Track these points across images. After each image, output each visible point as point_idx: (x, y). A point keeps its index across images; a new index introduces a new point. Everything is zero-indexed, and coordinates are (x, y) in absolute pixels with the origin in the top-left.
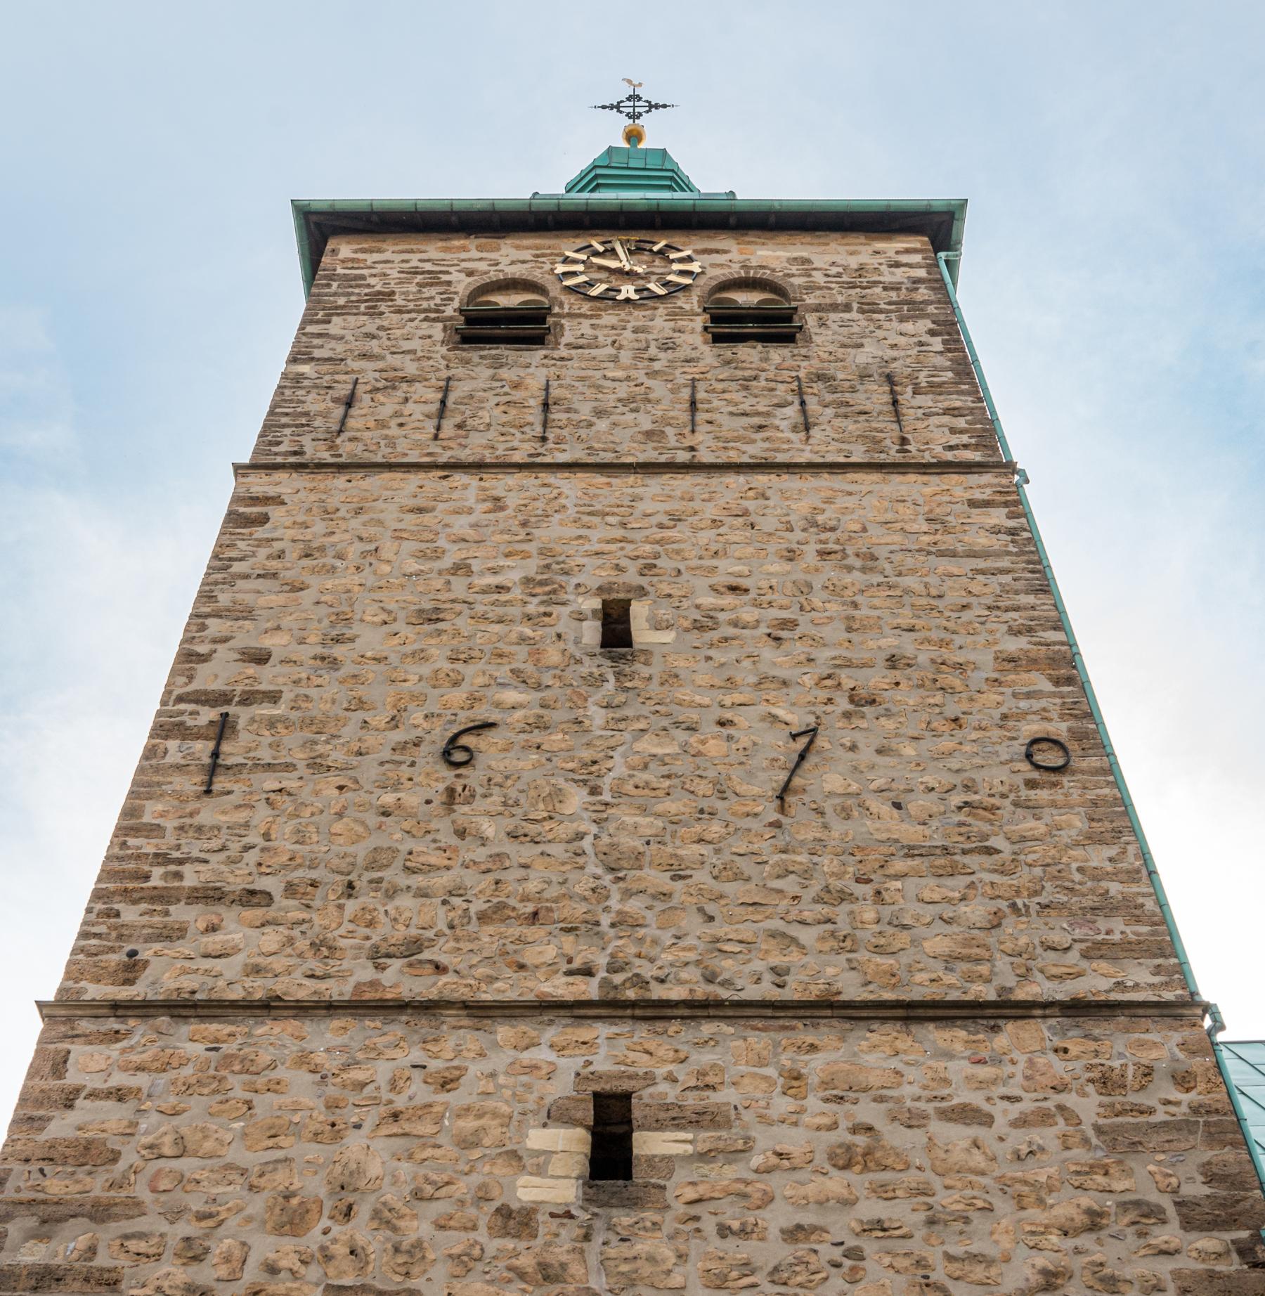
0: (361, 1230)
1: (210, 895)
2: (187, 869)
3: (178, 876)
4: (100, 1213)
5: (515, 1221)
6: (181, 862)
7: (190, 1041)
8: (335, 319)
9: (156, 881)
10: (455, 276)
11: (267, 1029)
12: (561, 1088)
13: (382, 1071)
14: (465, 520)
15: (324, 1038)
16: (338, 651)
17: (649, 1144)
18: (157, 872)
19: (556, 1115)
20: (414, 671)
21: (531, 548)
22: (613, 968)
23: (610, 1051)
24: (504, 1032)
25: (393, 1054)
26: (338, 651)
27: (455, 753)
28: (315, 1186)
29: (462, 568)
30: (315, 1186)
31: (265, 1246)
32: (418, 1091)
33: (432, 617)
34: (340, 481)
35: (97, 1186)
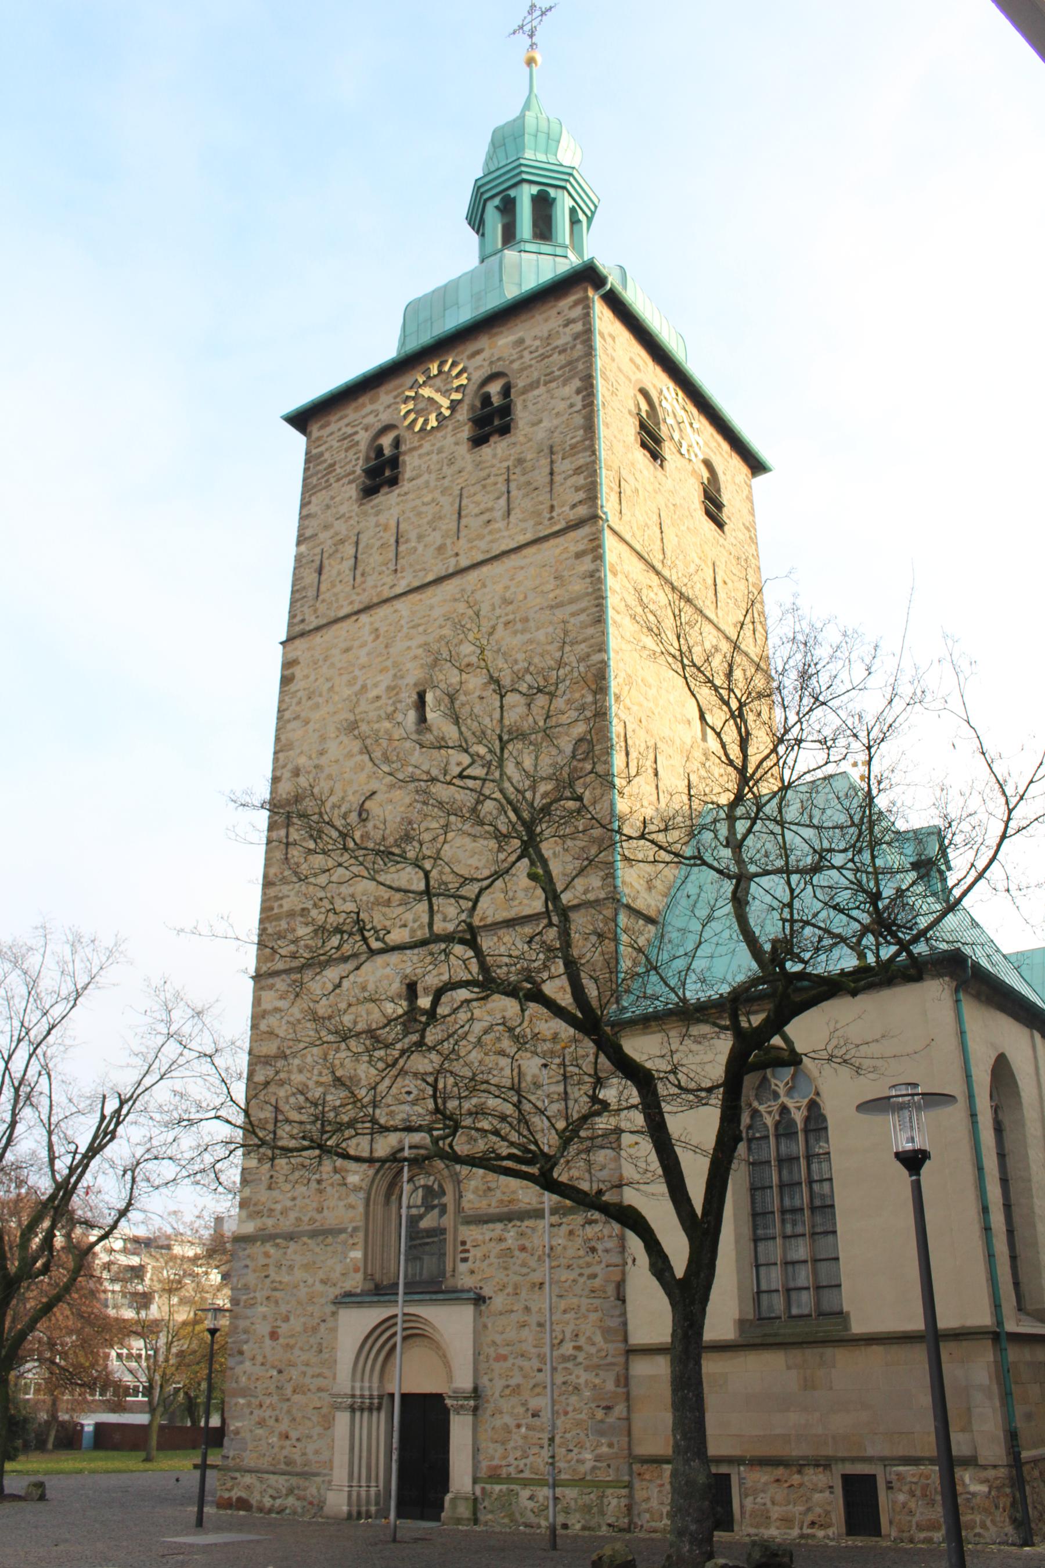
2: (284, 902)
3: (281, 906)
6: (281, 898)
8: (313, 499)
9: (276, 911)
14: (363, 652)
18: (276, 905)
21: (389, 663)
22: (415, 921)
26: (323, 761)
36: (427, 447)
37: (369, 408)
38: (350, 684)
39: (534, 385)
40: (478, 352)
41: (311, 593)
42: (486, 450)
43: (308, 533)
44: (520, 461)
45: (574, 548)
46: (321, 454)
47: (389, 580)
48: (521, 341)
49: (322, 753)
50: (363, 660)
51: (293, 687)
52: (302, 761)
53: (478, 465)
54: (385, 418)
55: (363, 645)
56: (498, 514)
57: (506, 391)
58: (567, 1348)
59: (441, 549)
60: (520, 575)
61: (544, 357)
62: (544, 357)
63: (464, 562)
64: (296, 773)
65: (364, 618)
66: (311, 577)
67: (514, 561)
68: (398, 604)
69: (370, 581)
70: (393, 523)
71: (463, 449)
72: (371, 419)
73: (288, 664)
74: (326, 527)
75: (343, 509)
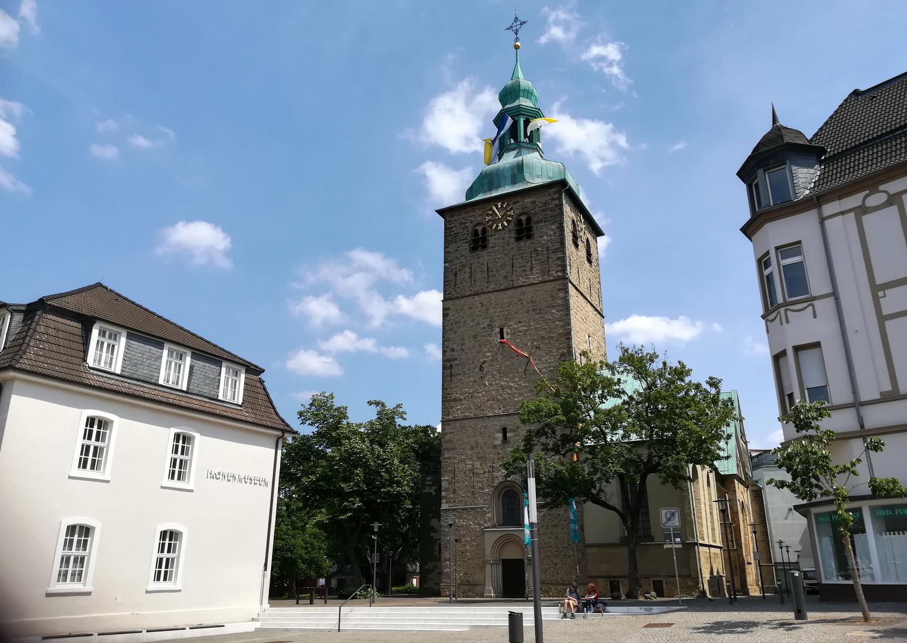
0: (479, 449)
1: (455, 400)
4: (453, 449)
5: (495, 447)
7: (457, 424)
10: (469, 224)
11: (466, 421)
12: (498, 428)
13: (479, 427)
15: (472, 422)
16: (463, 347)
17: (508, 435)
19: (498, 432)
23: (504, 422)
24: (492, 419)
25: (480, 424)
26: (463, 347)
28: (473, 444)
30: (473, 444)
31: (470, 452)
32: (483, 429)
33: (475, 337)
35: (452, 446)
36: (497, 236)
37: (472, 214)
38: (473, 321)
39: (541, 221)
40: (518, 202)
41: (453, 283)
42: (522, 243)
43: (449, 259)
44: (536, 250)
45: (557, 287)
46: (452, 228)
47: (486, 285)
48: (534, 202)
49: (463, 344)
50: (477, 313)
51: (448, 318)
52: (455, 346)
54: (479, 219)
55: (477, 307)
56: (528, 268)
57: (529, 220)
58: (566, 545)
59: (506, 277)
61: (543, 211)
62: (543, 211)
63: (516, 285)
64: (453, 350)
65: (476, 298)
66: (452, 277)
68: (490, 295)
69: (478, 284)
70: (485, 263)
71: (513, 240)
72: (472, 218)
73: (444, 309)
74: (457, 258)
75: (463, 253)
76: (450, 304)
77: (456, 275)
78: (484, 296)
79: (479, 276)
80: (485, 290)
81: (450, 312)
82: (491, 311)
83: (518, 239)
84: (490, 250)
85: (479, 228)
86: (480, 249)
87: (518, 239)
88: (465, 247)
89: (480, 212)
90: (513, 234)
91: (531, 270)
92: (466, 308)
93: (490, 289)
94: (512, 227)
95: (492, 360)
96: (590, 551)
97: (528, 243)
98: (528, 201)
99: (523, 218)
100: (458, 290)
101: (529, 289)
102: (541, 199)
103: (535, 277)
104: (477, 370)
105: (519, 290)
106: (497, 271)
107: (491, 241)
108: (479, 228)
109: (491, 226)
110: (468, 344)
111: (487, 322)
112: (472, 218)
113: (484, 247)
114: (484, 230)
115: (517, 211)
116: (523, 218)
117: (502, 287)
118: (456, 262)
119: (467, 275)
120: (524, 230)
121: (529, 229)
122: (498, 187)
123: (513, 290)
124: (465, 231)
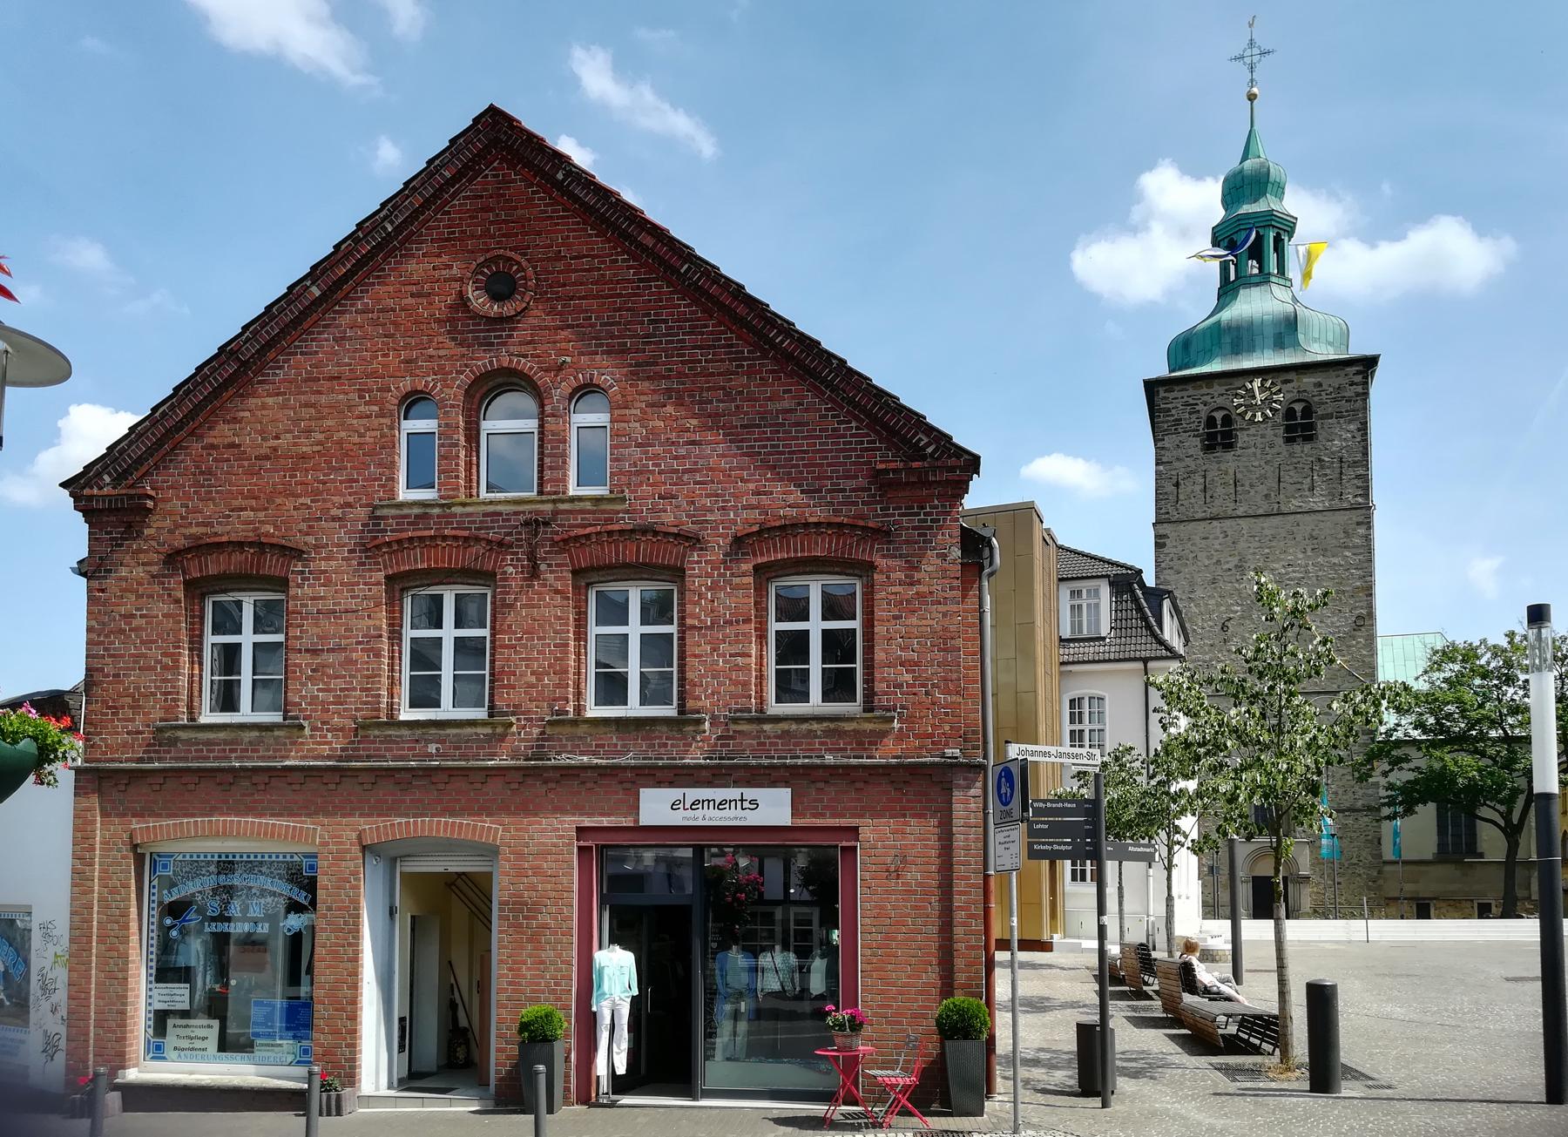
20: (1212, 602)
27: (1224, 628)
29: (1218, 562)
34: (1181, 526)
36: (1252, 431)
37: (1205, 391)
38: (1208, 558)
39: (1330, 416)
41: (1172, 498)
42: (1297, 448)
46: (1169, 410)
47: (1232, 505)
48: (1320, 385)
51: (1166, 550)
53: (1291, 455)
54: (1220, 401)
56: (1306, 487)
57: (1308, 412)
59: (1267, 496)
60: (1322, 525)
63: (1284, 509)
65: (1215, 523)
66: (1170, 488)
67: (1319, 517)
68: (1240, 521)
70: (1231, 472)
71: (1280, 441)
72: (1207, 398)
75: (1191, 452)
76: (1166, 529)
77: (1177, 485)
78: (1228, 522)
79: (1220, 490)
80: (1230, 512)
81: (1168, 541)
82: (1242, 545)
83: (1289, 441)
84: (1239, 452)
85: (1219, 415)
86: (1219, 448)
87: (1289, 440)
88: (1194, 444)
89: (1222, 390)
90: (1281, 431)
91: (1312, 489)
92: (1197, 539)
93: (1239, 513)
94: (1279, 419)
95: (1242, 617)
96: (1388, 868)
97: (1307, 447)
98: (1308, 381)
99: (1298, 407)
100: (1182, 509)
101: (1307, 517)
102: (1331, 380)
103: (1317, 501)
104: (1217, 629)
105: (1291, 517)
106: (1251, 486)
107: (1242, 438)
108: (1219, 415)
109: (1242, 415)
110: (1199, 593)
111: (1235, 561)
112: (1207, 398)
113: (1229, 446)
114: (1227, 420)
115: (1289, 396)
116: (1298, 407)
117: (1261, 511)
118: (1176, 464)
119: (1198, 488)
120: (1300, 425)
121: (1311, 427)
122: (1251, 349)
123: (1279, 518)
124: (1194, 417)
